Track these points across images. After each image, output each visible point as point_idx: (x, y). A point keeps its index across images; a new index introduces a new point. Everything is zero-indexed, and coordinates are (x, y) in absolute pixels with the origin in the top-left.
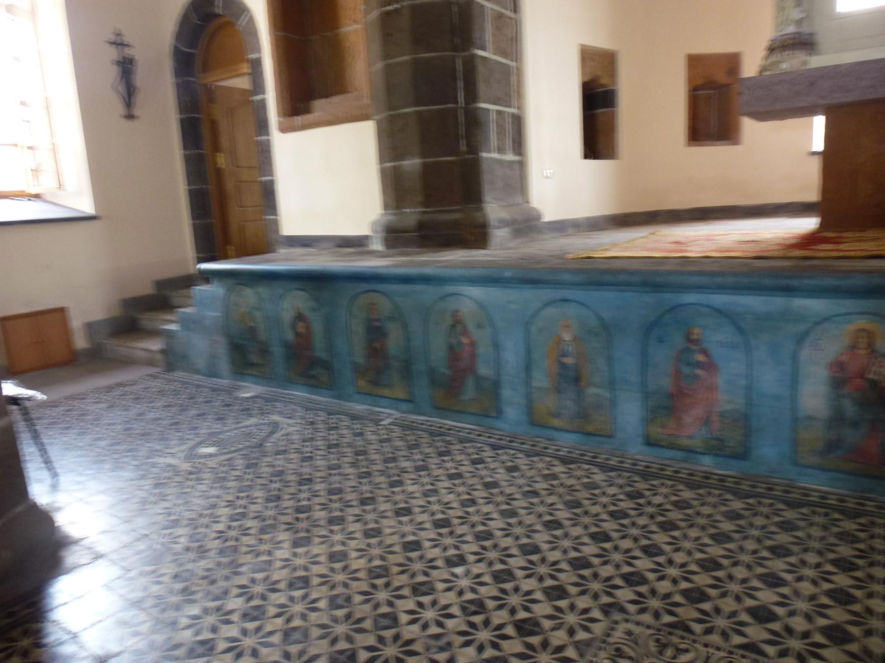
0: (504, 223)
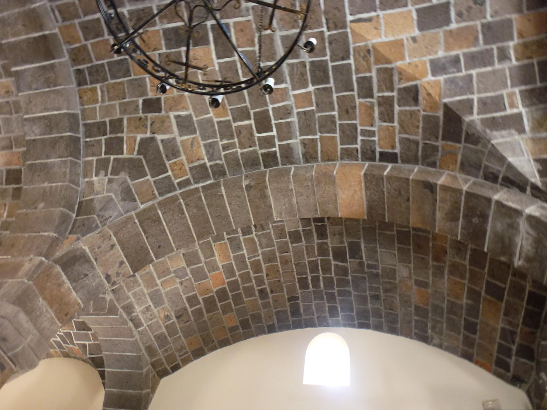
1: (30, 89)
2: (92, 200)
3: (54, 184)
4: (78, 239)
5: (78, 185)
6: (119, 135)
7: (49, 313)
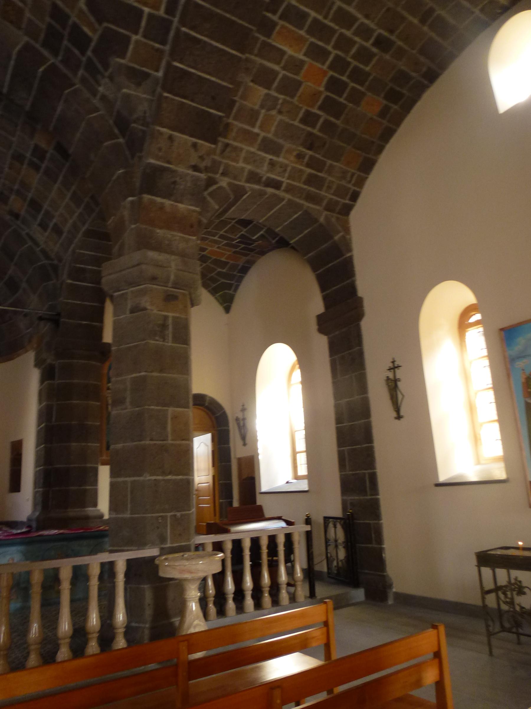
4: (140, 158)
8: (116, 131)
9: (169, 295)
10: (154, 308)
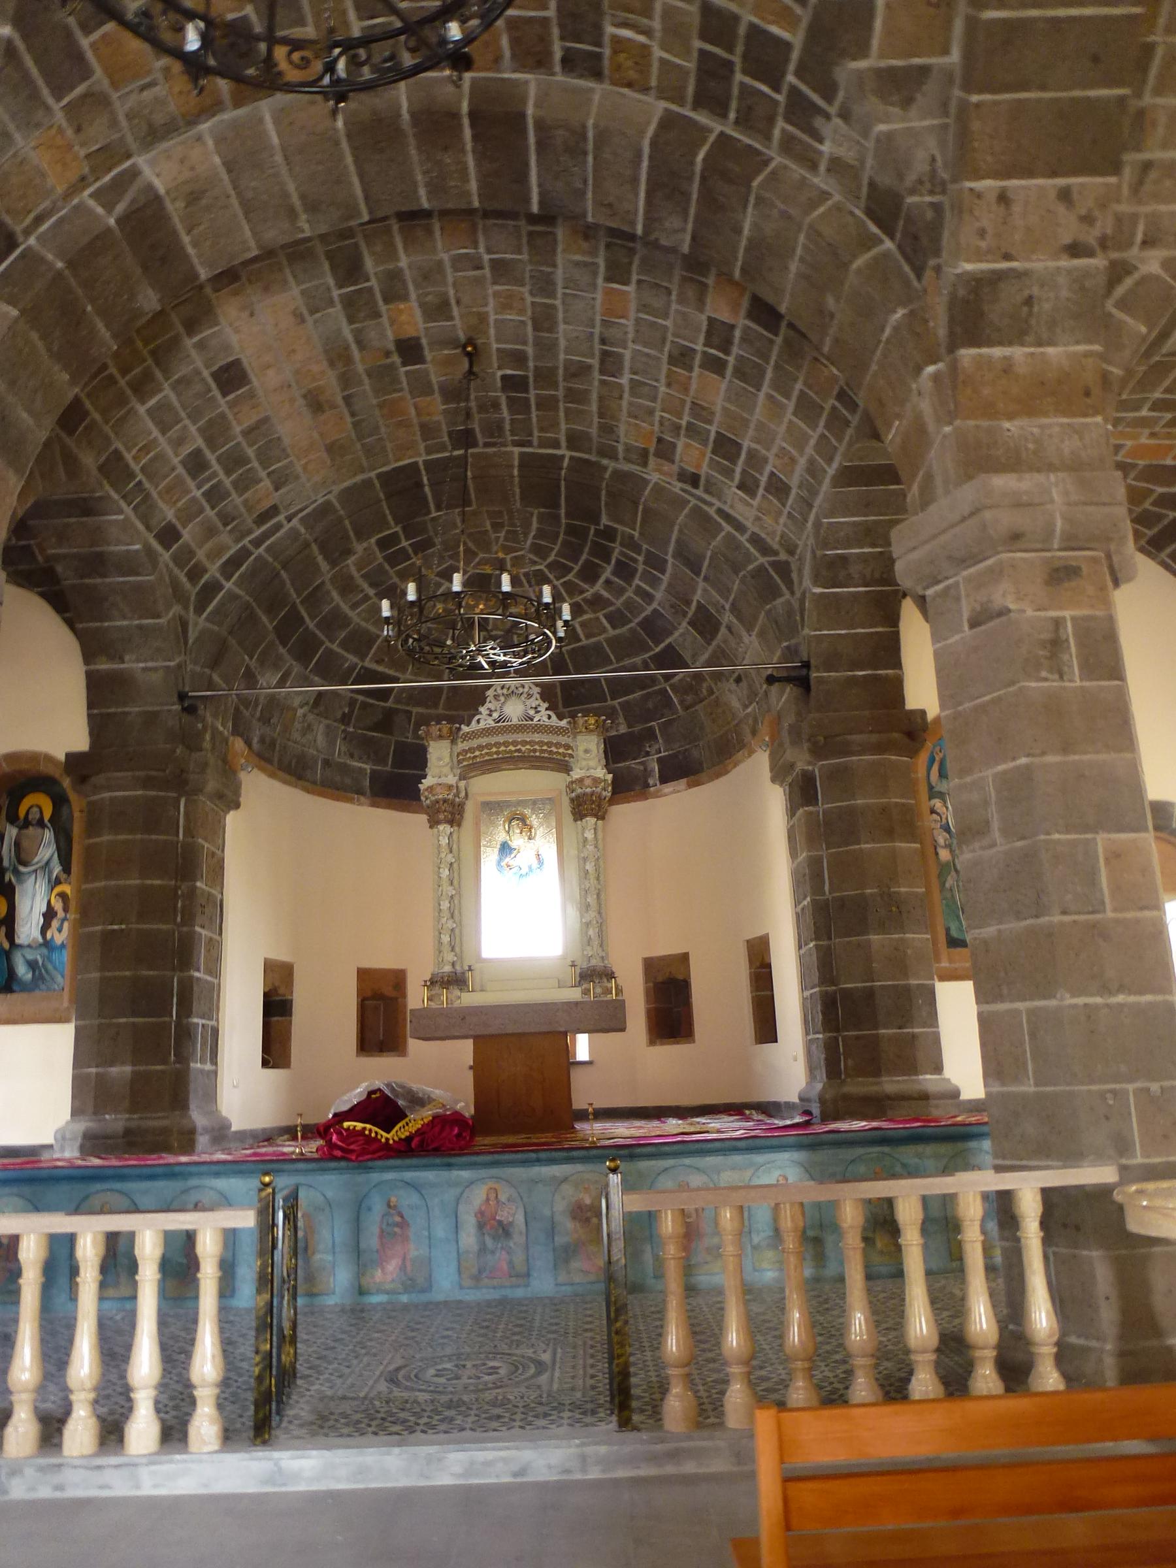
0: (206, 1130)
1: (582, 194)
2: (872, 185)
3: (799, 251)
4: (938, 269)
5: (825, 195)
6: (742, 30)
7: (1050, 426)
8: (874, 229)
9: (1057, 570)
10: (1026, 607)
